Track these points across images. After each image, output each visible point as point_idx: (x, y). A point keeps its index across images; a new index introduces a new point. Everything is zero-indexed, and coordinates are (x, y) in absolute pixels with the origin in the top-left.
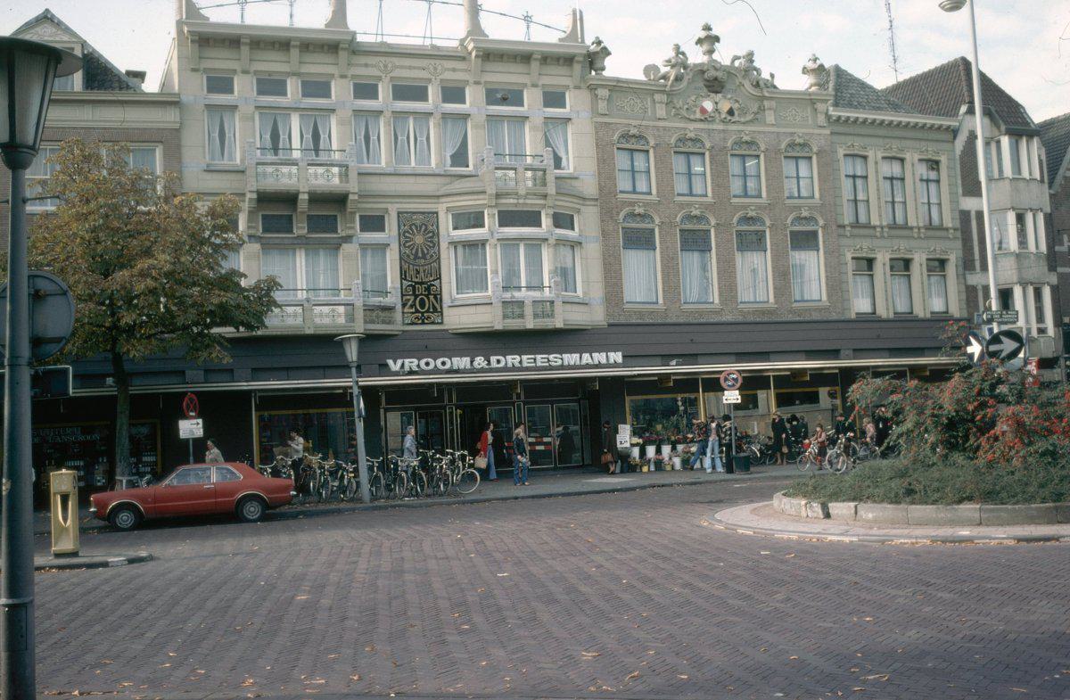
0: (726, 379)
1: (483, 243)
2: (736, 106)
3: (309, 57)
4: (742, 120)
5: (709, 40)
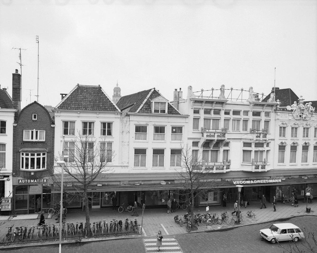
0: (307, 190)
1: (251, 151)
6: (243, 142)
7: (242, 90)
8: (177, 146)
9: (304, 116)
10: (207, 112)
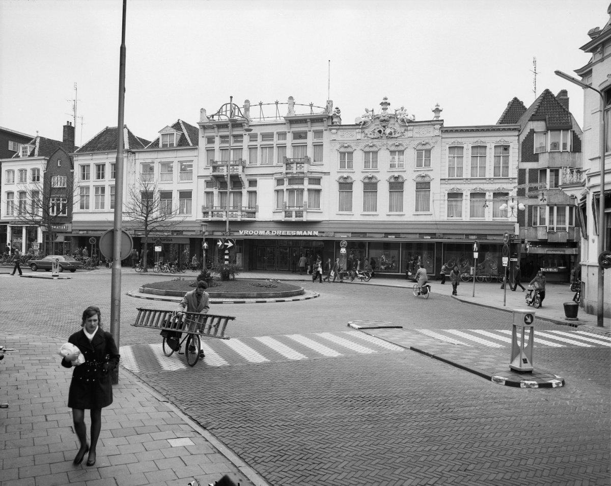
0: (342, 244)
2: (392, 131)
3: (315, 124)
4: (396, 136)
5: (385, 104)
6: (275, 179)
7: (277, 103)
8: (185, 187)
9: (388, 131)
10: (224, 138)
